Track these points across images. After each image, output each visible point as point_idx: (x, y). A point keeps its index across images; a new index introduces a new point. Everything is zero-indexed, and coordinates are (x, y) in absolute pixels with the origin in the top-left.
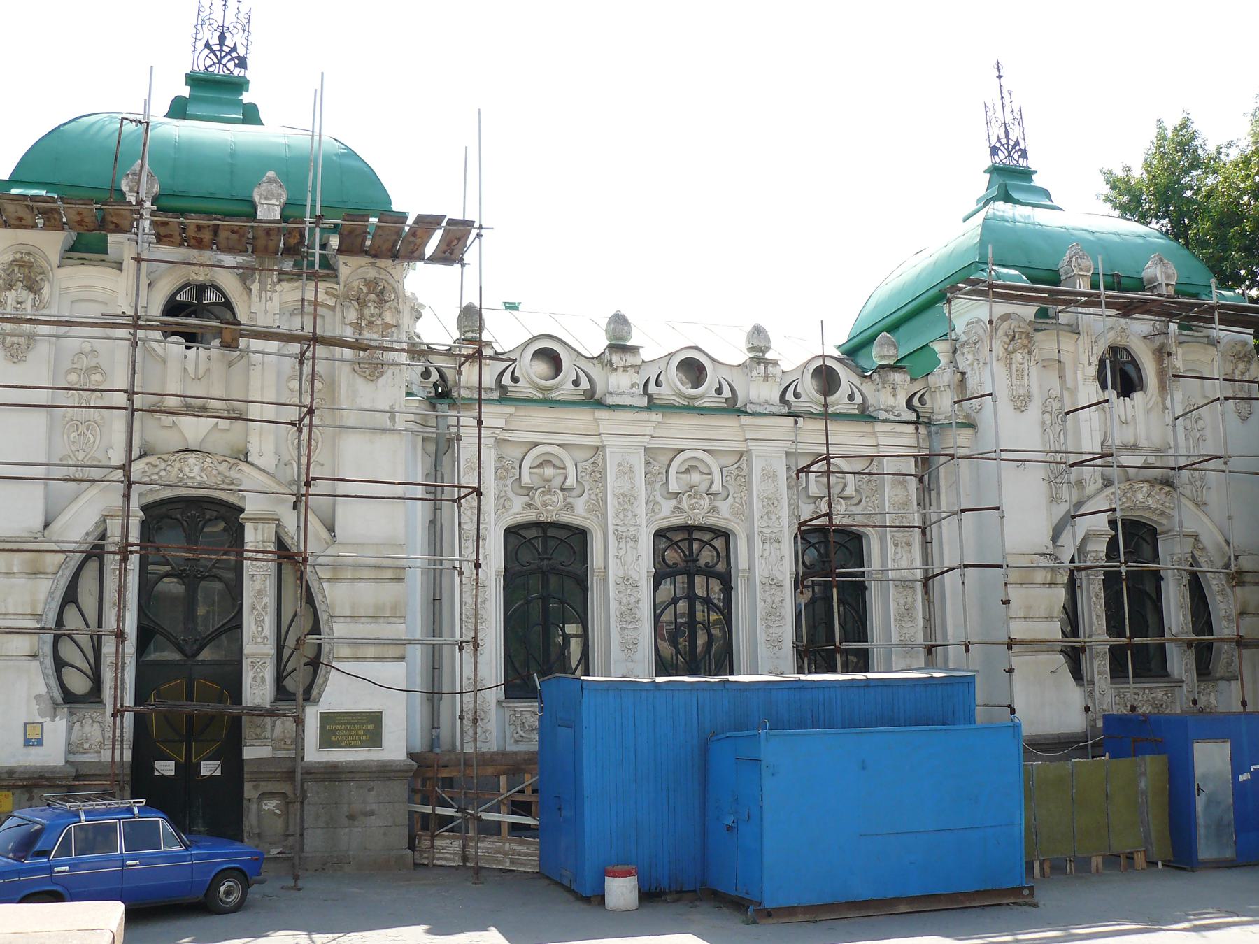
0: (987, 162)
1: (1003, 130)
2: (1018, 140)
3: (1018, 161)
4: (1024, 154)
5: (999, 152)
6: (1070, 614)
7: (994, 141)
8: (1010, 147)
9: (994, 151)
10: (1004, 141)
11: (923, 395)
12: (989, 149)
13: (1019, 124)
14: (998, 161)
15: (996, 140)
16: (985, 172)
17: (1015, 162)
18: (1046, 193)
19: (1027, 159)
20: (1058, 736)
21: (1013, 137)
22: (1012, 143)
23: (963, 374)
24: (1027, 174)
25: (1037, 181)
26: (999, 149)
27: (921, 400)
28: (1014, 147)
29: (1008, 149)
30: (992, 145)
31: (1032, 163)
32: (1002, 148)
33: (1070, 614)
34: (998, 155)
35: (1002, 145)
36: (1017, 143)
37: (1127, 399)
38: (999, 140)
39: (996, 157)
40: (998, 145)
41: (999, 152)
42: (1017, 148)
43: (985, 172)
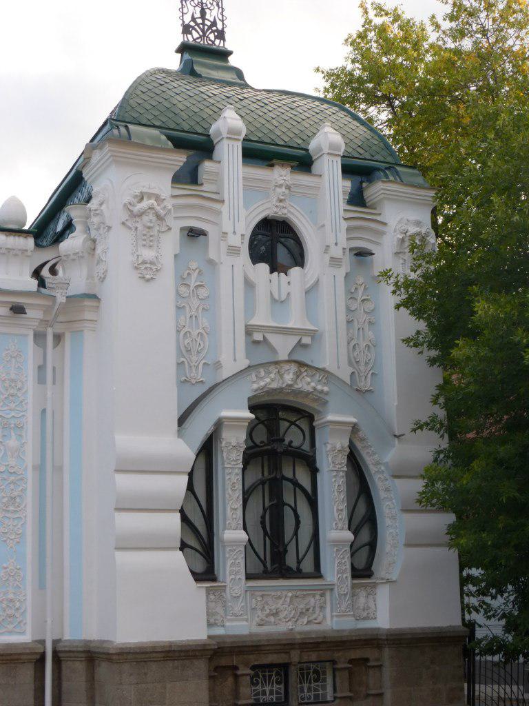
0: (179, 39)
1: (198, 9)
2: (215, 19)
3: (213, 42)
4: (221, 35)
5: (194, 32)
6: (204, 508)
7: (187, 19)
8: (206, 27)
9: (186, 29)
10: (199, 21)
11: (55, 265)
12: (181, 28)
13: (218, 5)
14: (191, 39)
15: (190, 19)
16: (178, 51)
17: (210, 43)
18: (239, 73)
19: (224, 41)
20: (171, 644)
21: (210, 16)
22: (208, 23)
23: (94, 241)
24: (224, 55)
25: (233, 61)
26: (193, 28)
27: (53, 271)
28: (210, 27)
29: (203, 30)
30: (187, 22)
31: (229, 45)
32: (196, 27)
33: (204, 508)
34: (191, 33)
35: (197, 24)
36: (214, 23)
37: (282, 275)
38: (193, 19)
39: (189, 36)
40: (192, 24)
41: (194, 32)
42: (214, 28)
43: (178, 51)
